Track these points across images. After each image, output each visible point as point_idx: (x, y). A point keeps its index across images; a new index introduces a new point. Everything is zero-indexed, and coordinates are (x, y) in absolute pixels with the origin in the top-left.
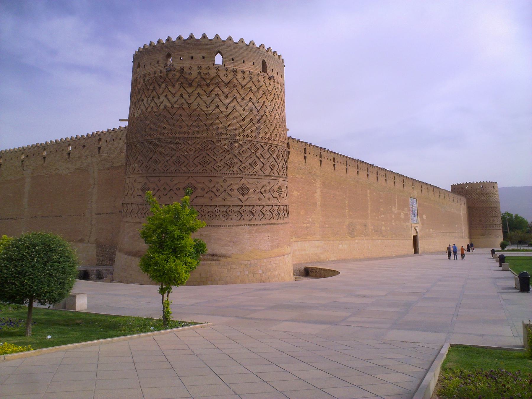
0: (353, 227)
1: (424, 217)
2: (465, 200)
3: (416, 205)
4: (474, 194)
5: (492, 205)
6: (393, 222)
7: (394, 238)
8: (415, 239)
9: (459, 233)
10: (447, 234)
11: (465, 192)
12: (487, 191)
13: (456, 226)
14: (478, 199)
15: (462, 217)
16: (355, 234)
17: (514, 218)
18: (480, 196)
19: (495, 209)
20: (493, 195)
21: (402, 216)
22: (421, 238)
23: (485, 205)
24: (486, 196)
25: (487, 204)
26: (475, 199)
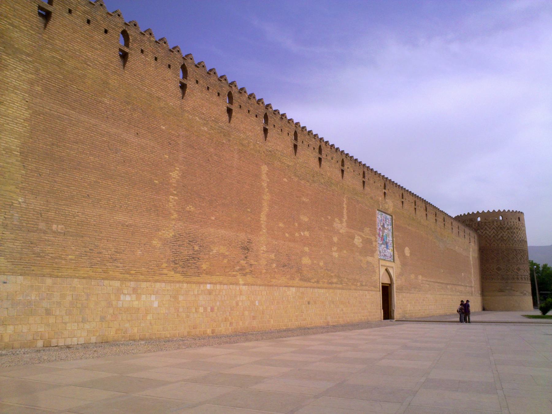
0: (197, 248)
1: (407, 251)
2: (476, 237)
3: (390, 227)
4: (490, 228)
5: (517, 246)
6: (335, 251)
7: (334, 285)
8: (387, 291)
9: (466, 286)
10: (448, 287)
11: (475, 226)
12: (509, 224)
13: (463, 274)
14: (496, 236)
15: (472, 262)
16: (204, 266)
17: (541, 269)
18: (499, 232)
19: (521, 252)
20: (518, 230)
21: (358, 241)
22: (400, 289)
23: (506, 245)
24: (508, 232)
25: (509, 245)
26: (490, 237)
